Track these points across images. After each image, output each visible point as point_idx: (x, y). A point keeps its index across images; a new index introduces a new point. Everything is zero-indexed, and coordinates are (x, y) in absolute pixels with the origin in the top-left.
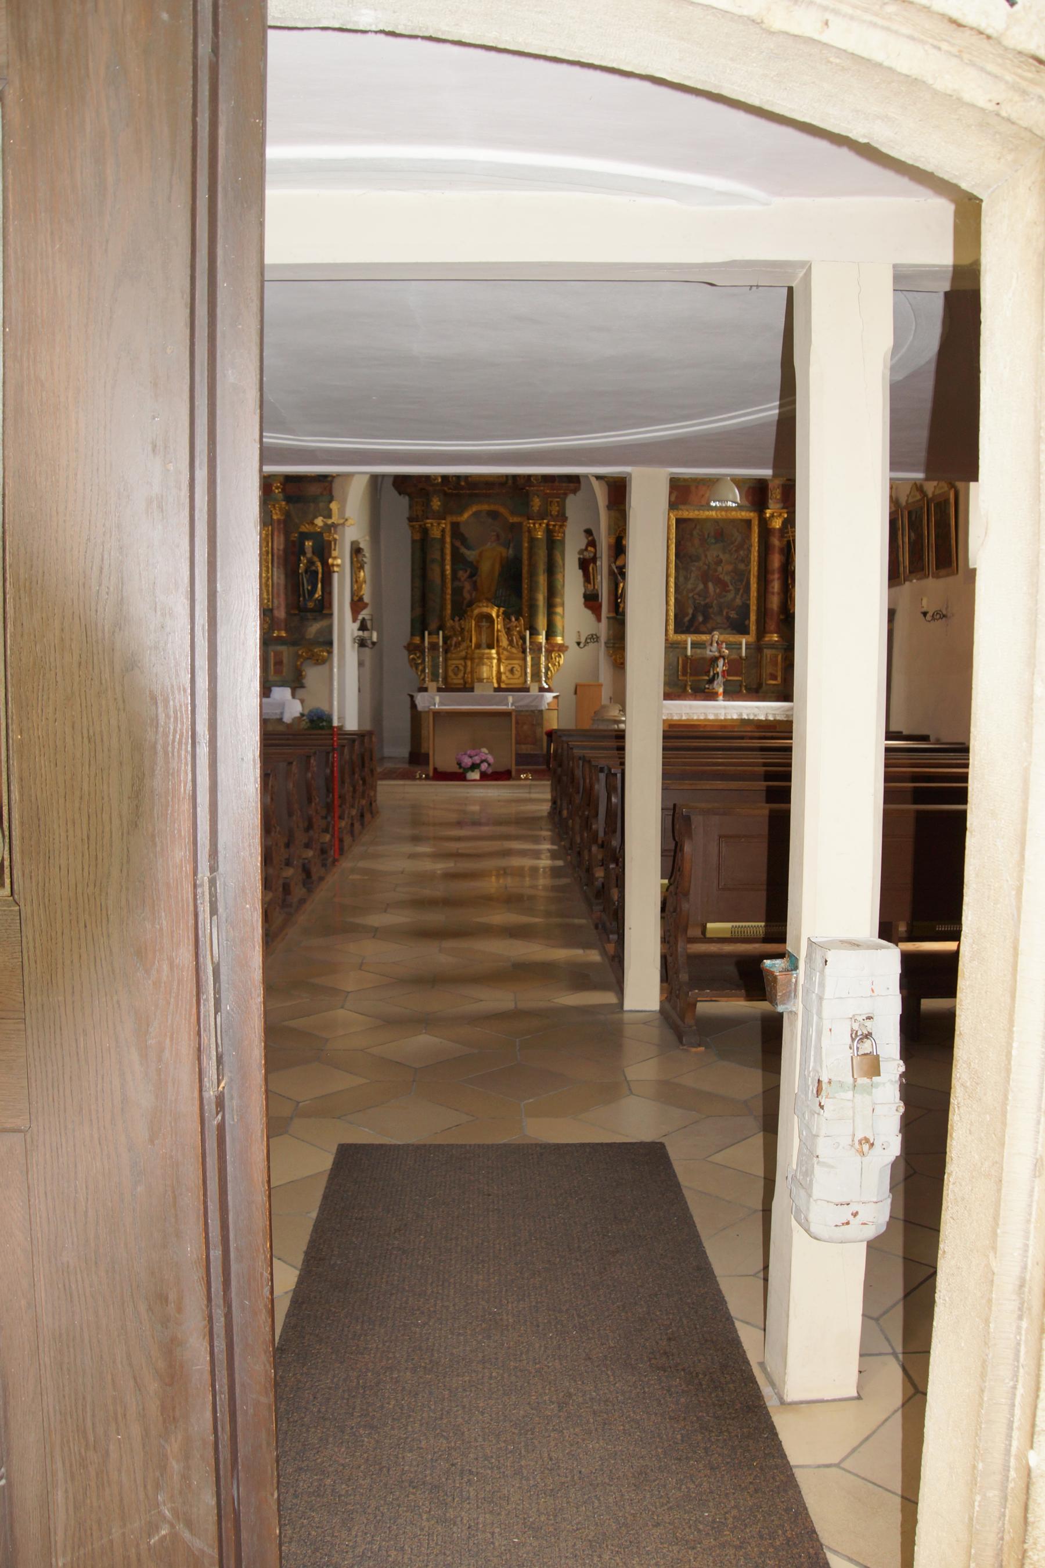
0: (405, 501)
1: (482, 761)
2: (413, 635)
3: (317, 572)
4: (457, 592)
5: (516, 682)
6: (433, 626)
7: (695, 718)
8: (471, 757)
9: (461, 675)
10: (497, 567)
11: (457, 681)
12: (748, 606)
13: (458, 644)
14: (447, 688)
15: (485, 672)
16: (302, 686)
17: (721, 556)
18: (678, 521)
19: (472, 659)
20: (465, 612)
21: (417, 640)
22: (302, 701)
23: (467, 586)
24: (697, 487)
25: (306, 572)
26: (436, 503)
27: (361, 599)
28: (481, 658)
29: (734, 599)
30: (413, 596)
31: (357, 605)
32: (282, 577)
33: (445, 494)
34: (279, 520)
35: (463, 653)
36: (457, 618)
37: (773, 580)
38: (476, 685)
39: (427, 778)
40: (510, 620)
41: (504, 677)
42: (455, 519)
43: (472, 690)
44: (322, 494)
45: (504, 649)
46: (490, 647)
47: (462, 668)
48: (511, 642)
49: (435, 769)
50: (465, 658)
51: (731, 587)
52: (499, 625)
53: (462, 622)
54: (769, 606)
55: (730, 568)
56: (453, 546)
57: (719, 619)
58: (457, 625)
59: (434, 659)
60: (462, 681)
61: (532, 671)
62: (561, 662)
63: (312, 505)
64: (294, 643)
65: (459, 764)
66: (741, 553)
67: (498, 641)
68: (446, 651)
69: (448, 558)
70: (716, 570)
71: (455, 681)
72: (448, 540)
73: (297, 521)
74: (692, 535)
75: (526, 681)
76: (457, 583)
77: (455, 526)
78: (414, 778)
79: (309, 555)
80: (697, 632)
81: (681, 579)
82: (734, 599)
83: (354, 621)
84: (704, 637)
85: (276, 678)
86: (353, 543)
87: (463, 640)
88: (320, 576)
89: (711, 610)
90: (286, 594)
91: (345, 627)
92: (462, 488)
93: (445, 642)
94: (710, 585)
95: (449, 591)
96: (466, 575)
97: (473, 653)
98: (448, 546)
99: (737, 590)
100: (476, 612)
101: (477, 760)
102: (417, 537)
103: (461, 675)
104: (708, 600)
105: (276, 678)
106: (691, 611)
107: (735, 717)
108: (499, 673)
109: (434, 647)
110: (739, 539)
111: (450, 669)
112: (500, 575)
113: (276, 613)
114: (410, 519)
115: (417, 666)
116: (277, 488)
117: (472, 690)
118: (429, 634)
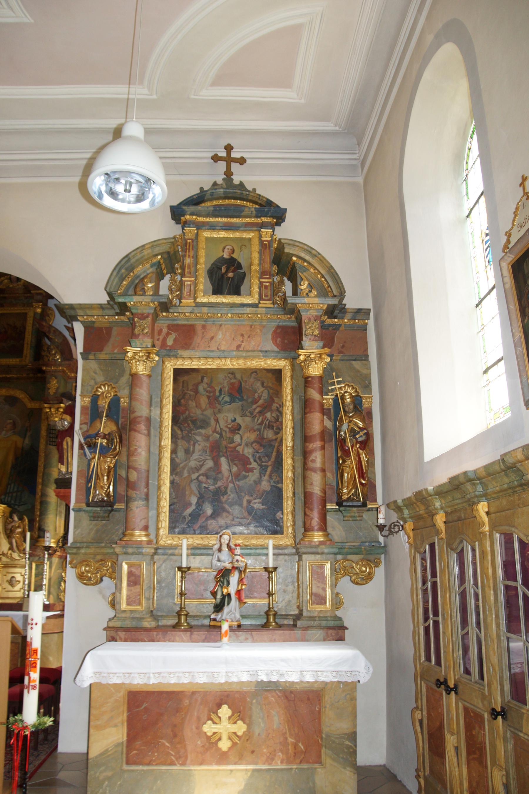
7: (173, 681)
10: (11, 458)
12: (280, 491)
17: (239, 420)
18: (178, 372)
24: (204, 327)
29: (258, 482)
37: (312, 451)
51: (254, 465)
54: (309, 489)
55: (253, 437)
57: (236, 510)
61: (35, 581)
66: (268, 415)
70: (232, 441)
74: (197, 392)
80: (204, 530)
81: (181, 454)
82: (258, 482)
84: (212, 540)
89: (224, 499)
94: (223, 460)
99: (263, 469)
104: (219, 484)
106: (194, 500)
107: (245, 678)
110: (265, 396)
112: (13, 467)
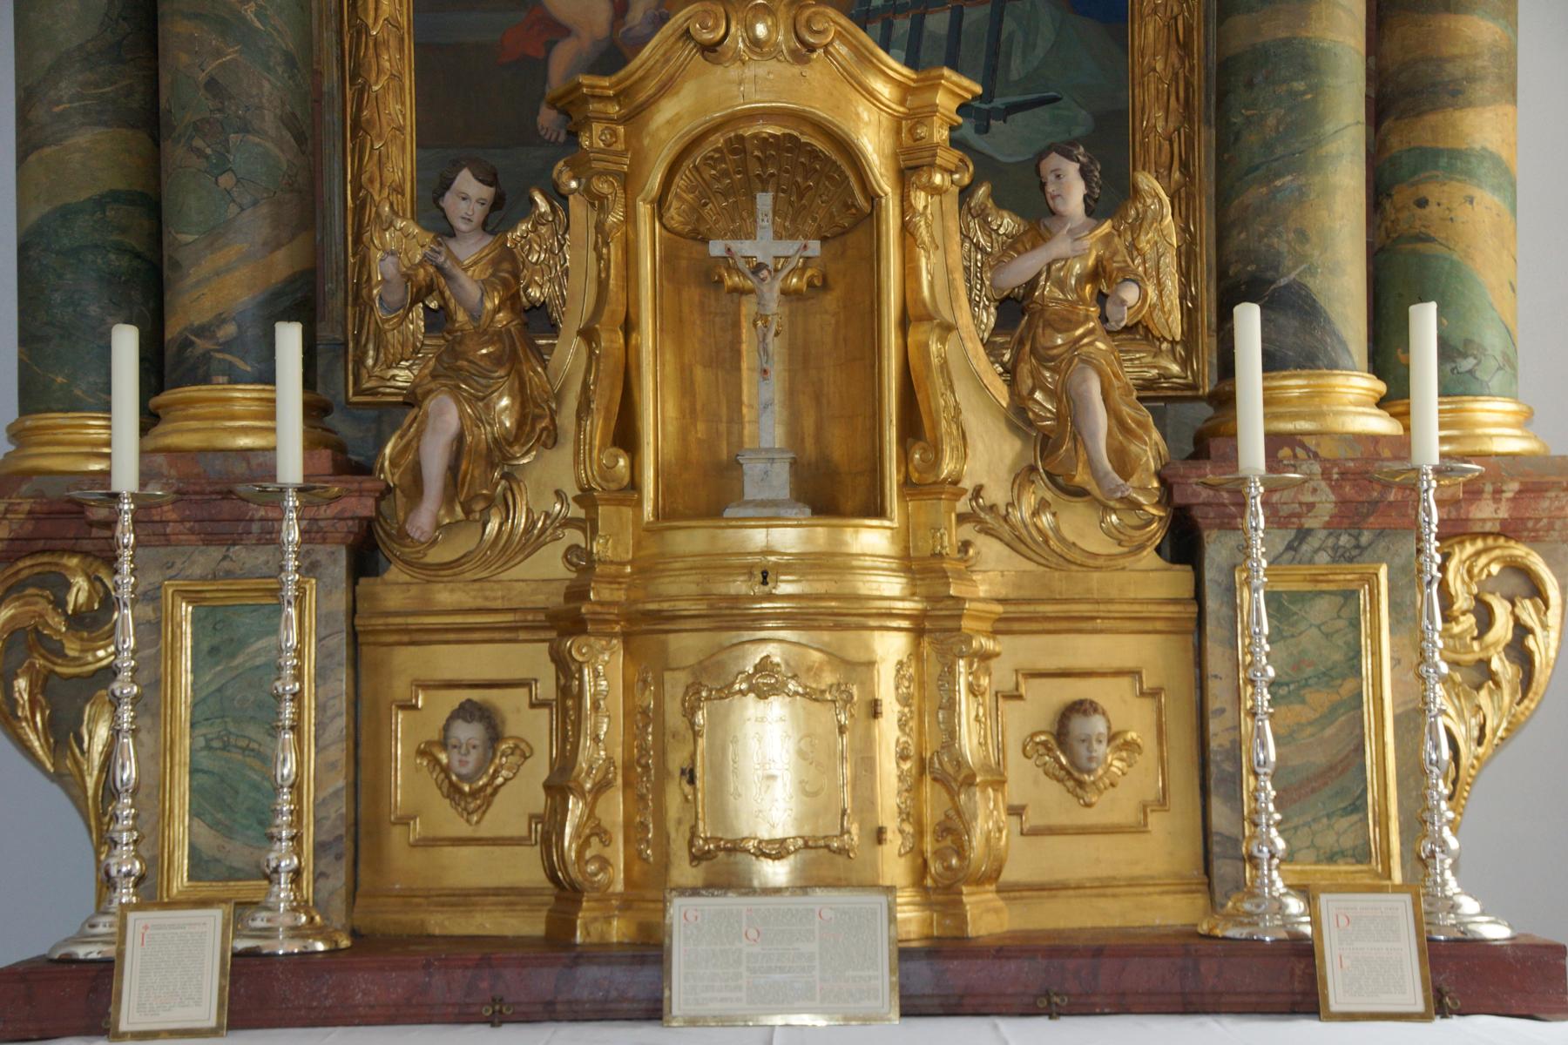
5: (1112, 860)
6: (223, 274)
9: (521, 796)
11: (475, 864)
13: (482, 474)
15: (767, 764)
20: (574, 112)
28: (733, 617)
35: (550, 564)
36: (468, 194)
38: (691, 922)
40: (1039, 215)
41: (986, 818)
45: (981, 517)
46: (831, 492)
47: (531, 726)
48: (1049, 450)
50: (566, 622)
52: (933, 255)
58: (470, 250)
60: (526, 869)
62: (1544, 646)
67: (913, 425)
71: (468, 868)
75: (1215, 862)
87: (536, 425)
100: (672, 118)
108: (938, 769)
109: (212, 503)
111: (401, 741)
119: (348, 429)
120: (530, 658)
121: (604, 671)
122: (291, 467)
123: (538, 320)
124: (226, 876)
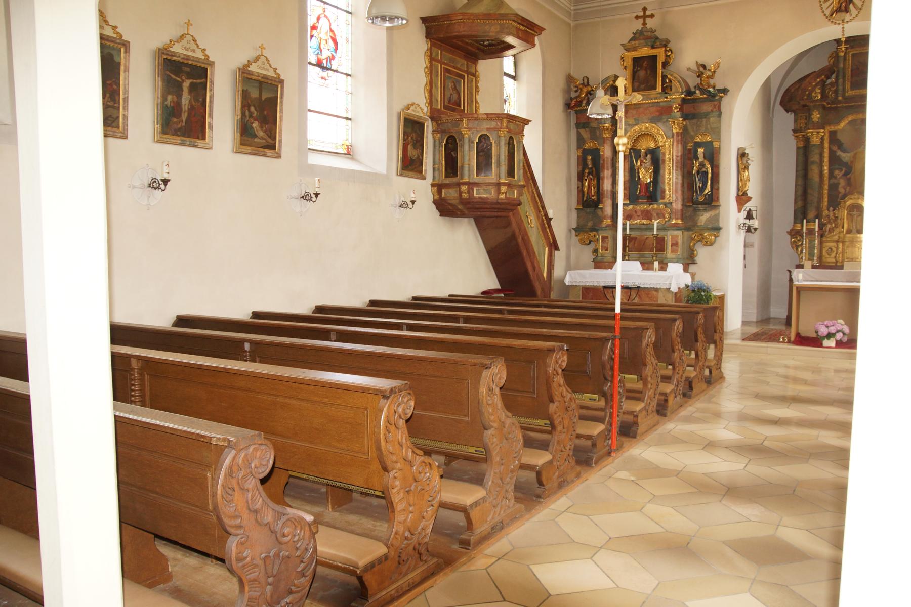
0: (791, 117)
1: (838, 331)
2: (795, 223)
3: (707, 173)
4: (833, 187)
6: (811, 215)
8: (827, 327)
9: (833, 255)
11: (831, 259)
13: (831, 230)
14: (821, 265)
16: (694, 263)
19: (843, 242)
20: (840, 203)
21: (798, 227)
22: (693, 276)
23: (842, 182)
25: (698, 172)
26: (816, 116)
27: (745, 194)
30: (796, 192)
31: (742, 198)
32: (680, 177)
33: (824, 107)
34: (677, 133)
35: (836, 238)
36: (831, 209)
38: (846, 263)
39: (789, 342)
42: (832, 128)
43: (842, 267)
44: (712, 111)
47: (834, 249)
49: (798, 335)
50: (837, 242)
53: (836, 212)
56: (830, 149)
58: (831, 214)
59: (811, 242)
63: (704, 120)
64: (688, 229)
65: (817, 332)
68: (822, 236)
69: (826, 160)
71: (829, 260)
72: (826, 145)
73: (692, 133)
76: (832, 181)
77: (833, 134)
78: (778, 341)
79: (701, 159)
83: (740, 211)
85: (674, 256)
86: (739, 149)
87: (836, 226)
88: (710, 175)
90: (683, 192)
91: (731, 215)
92: (840, 102)
93: (820, 228)
95: (826, 187)
96: (841, 175)
97: (844, 237)
98: (826, 151)
100: (848, 203)
101: (832, 330)
102: (801, 145)
103: (833, 255)
105: (674, 256)
109: (811, 232)
113: (674, 205)
114: (795, 131)
115: (797, 247)
116: (676, 108)
117: (842, 267)
118: (807, 222)
119: (821, 226)
120: (835, 244)
121: (840, 245)
122: (817, 229)
123: (836, 218)
124: (811, 258)
